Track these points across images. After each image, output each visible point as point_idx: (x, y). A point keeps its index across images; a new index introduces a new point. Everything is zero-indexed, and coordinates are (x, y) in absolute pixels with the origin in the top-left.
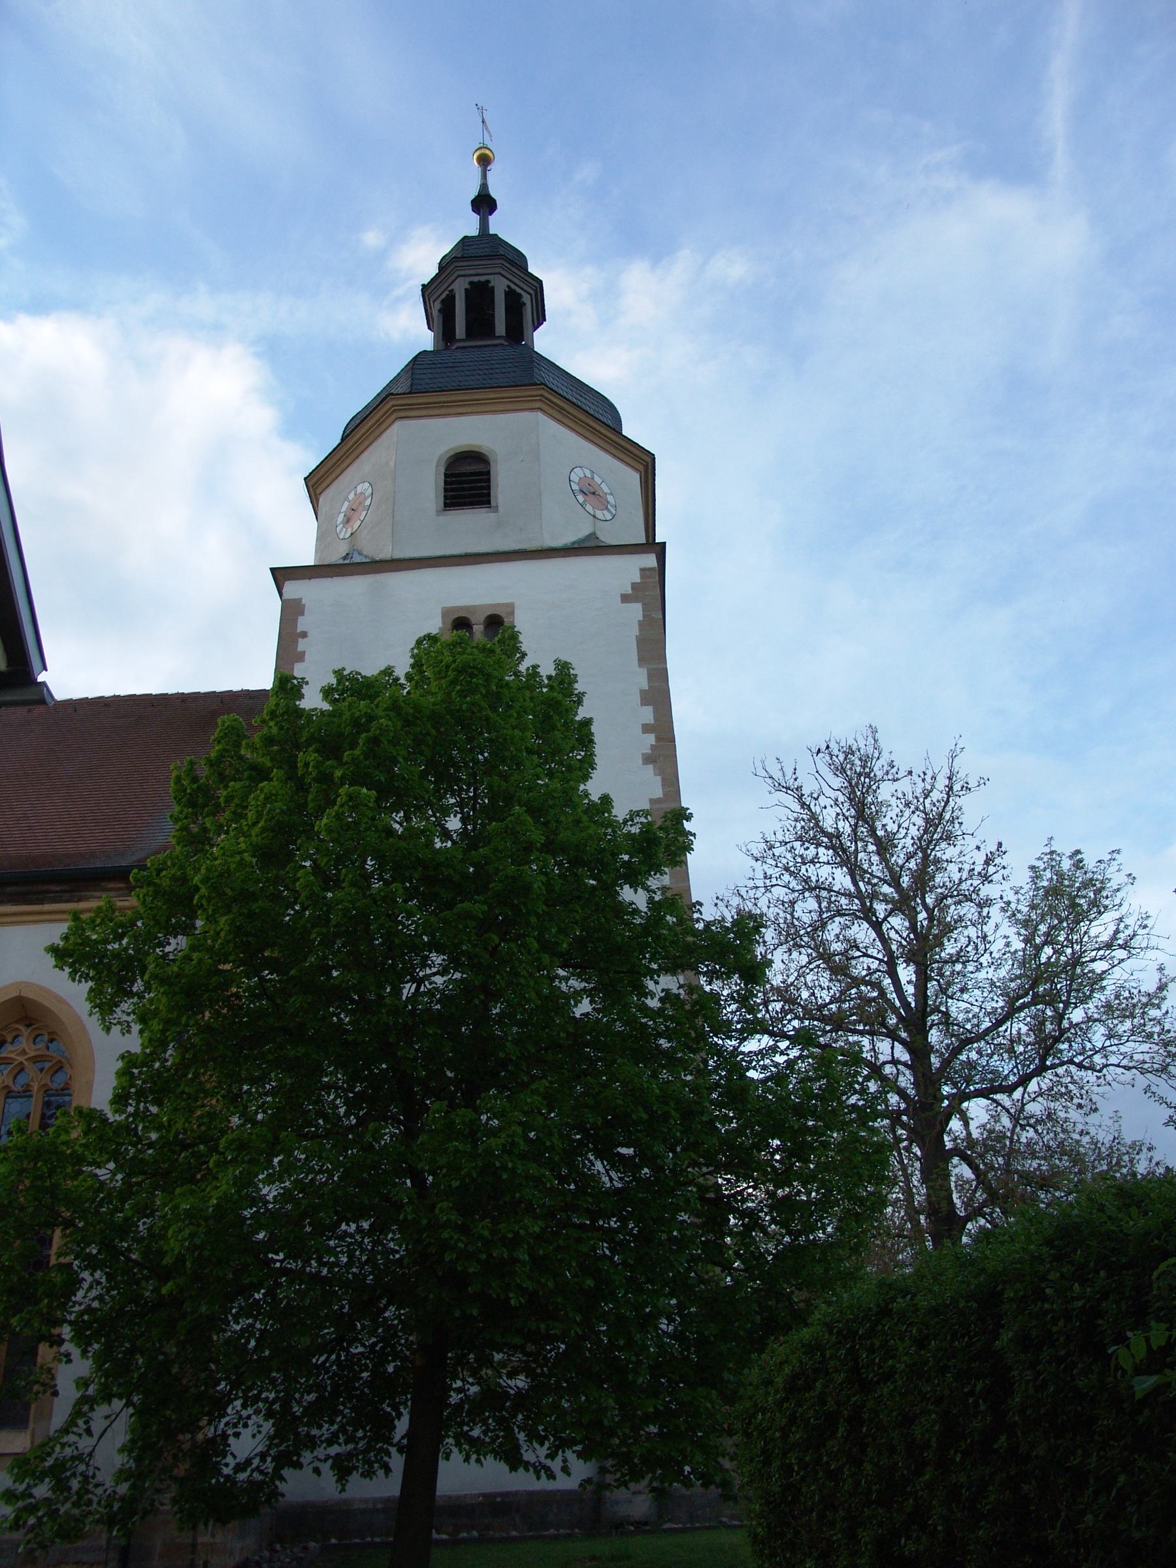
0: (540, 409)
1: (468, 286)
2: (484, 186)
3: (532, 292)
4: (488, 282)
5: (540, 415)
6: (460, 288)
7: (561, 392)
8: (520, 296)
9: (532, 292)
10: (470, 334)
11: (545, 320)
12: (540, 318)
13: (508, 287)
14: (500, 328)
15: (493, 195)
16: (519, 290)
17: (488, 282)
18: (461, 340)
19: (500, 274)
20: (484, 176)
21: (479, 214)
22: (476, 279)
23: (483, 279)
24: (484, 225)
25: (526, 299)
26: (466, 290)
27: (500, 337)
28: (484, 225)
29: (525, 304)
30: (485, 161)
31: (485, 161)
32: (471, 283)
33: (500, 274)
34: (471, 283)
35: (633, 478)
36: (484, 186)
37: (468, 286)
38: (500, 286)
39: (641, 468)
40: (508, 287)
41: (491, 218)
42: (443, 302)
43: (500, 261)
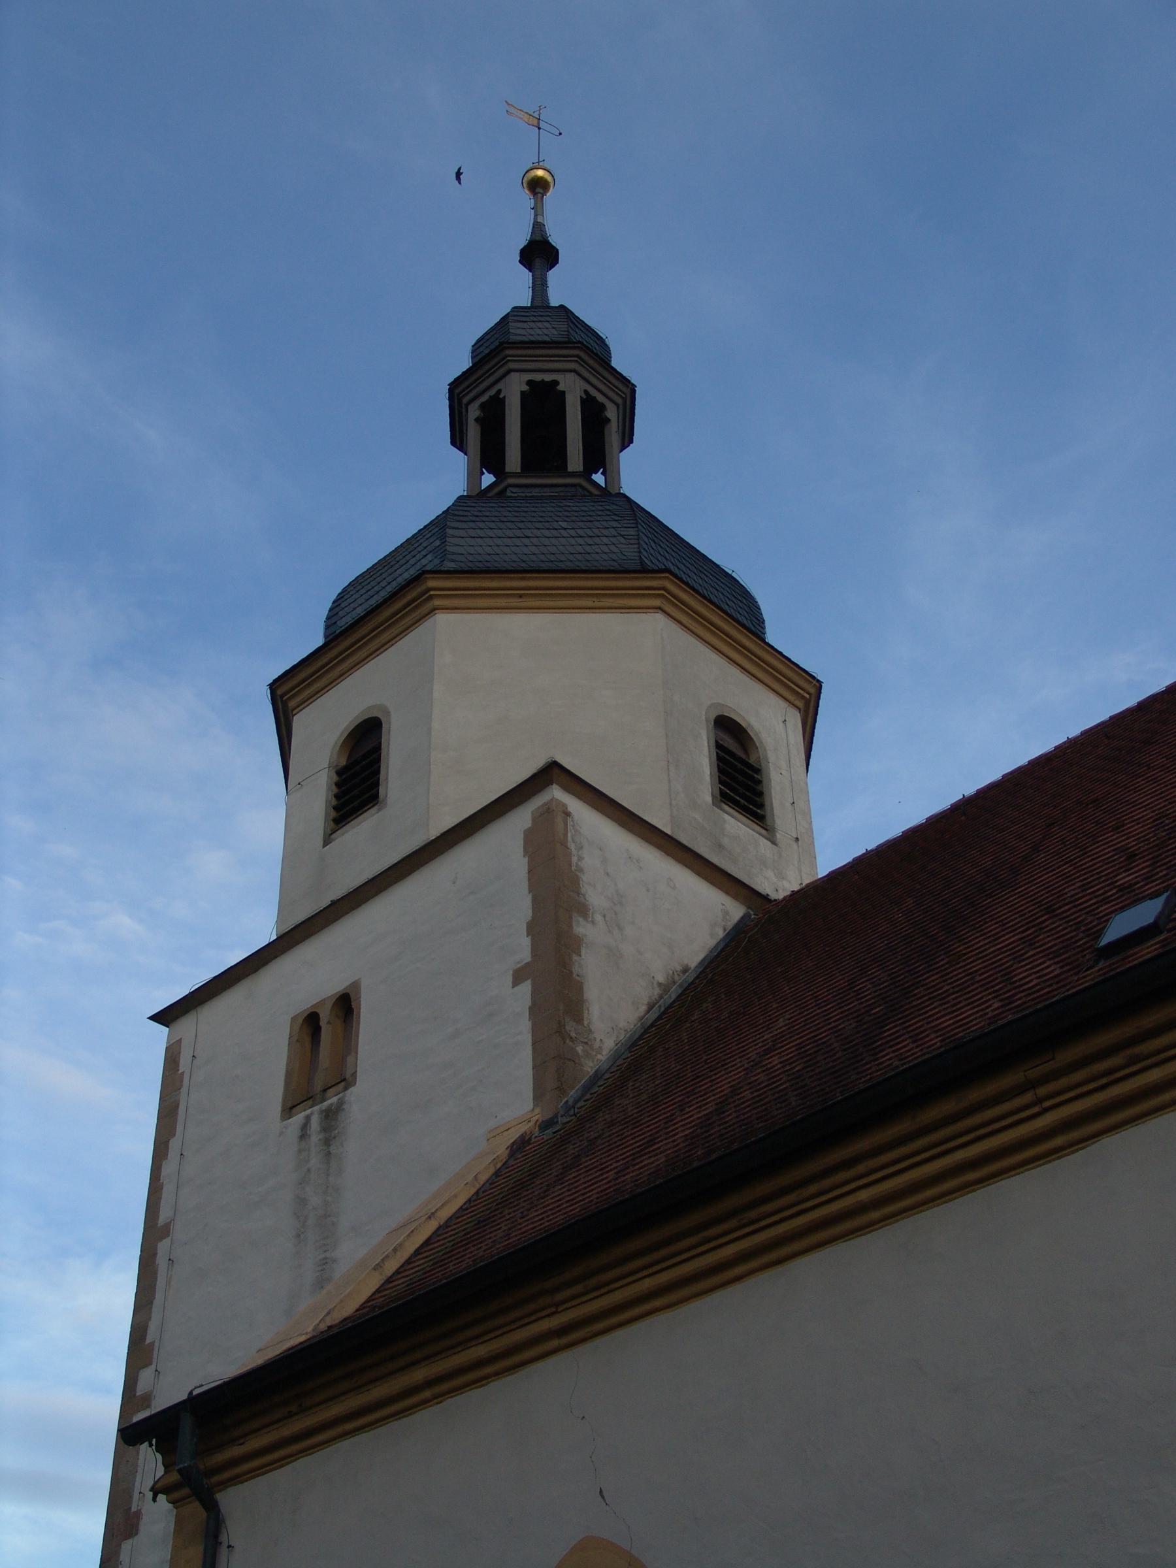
0: (660, 608)
1: (526, 388)
2: (538, 227)
3: (619, 401)
4: (556, 383)
5: (660, 617)
6: (514, 388)
7: (726, 608)
8: (602, 407)
9: (619, 401)
10: (530, 465)
11: (631, 441)
12: (627, 439)
13: (586, 392)
14: (575, 461)
15: (553, 240)
16: (601, 398)
17: (556, 383)
18: (514, 475)
19: (574, 371)
20: (538, 210)
21: (530, 271)
22: (538, 377)
23: (548, 378)
24: (539, 288)
25: (611, 413)
26: (523, 393)
27: (574, 474)
28: (539, 288)
29: (608, 420)
30: (537, 187)
31: (537, 187)
32: (530, 383)
33: (574, 371)
34: (529, 383)
35: (795, 720)
36: (538, 227)
37: (526, 388)
38: (572, 388)
39: (800, 704)
40: (586, 392)
41: (553, 275)
42: (483, 406)
43: (576, 352)
